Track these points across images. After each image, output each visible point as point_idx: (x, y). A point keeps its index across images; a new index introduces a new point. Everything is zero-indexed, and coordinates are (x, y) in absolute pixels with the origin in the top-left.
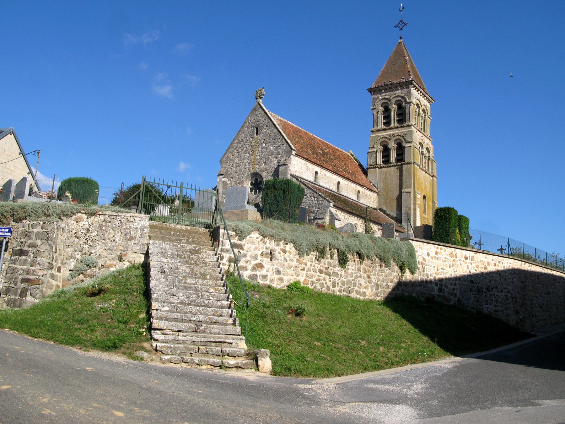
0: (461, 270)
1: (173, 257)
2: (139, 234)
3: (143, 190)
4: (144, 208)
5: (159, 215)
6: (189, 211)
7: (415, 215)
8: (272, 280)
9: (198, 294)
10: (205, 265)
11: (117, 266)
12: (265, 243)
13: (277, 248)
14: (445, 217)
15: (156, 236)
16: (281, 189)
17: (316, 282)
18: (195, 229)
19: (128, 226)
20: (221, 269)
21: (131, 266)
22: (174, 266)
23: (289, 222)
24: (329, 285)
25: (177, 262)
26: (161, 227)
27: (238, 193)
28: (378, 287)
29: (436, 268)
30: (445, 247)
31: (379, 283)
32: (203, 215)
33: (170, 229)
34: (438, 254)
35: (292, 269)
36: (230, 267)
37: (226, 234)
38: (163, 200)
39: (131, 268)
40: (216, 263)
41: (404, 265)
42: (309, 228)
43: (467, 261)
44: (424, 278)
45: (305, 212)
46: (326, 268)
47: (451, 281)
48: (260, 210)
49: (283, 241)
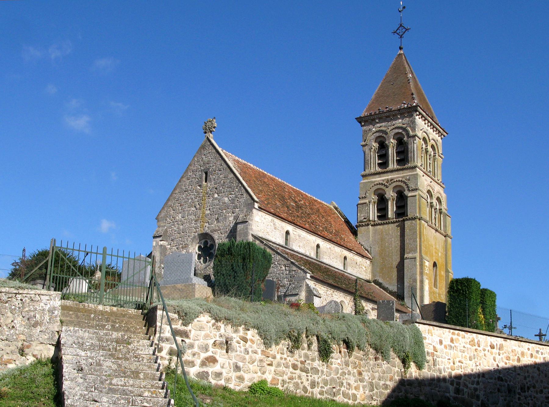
0: (485, 364)
1: (93, 349)
2: (47, 318)
3: (52, 257)
4: (53, 282)
5: (74, 292)
6: (115, 287)
7: (423, 289)
8: (229, 379)
9: (128, 400)
10: (137, 359)
11: (17, 362)
12: (218, 328)
13: (234, 335)
14: (463, 291)
15: (70, 321)
16: (240, 255)
17: (288, 381)
18: (124, 311)
19: (31, 307)
20: (159, 365)
21: (36, 361)
22: (94, 361)
23: (251, 301)
24: (306, 386)
25: (100, 355)
26: (77, 308)
27: (182, 261)
28: (373, 387)
29: (451, 361)
30: (463, 333)
31: (374, 381)
32: (134, 292)
33: (89, 312)
34: (454, 342)
35: (255, 364)
36: (171, 362)
37: (165, 316)
38: (79, 271)
39: (36, 364)
40: (152, 357)
41: (407, 356)
42: (279, 308)
43: (494, 351)
44: (435, 374)
45: (272, 286)
46: (302, 363)
47: (472, 378)
48: (211, 284)
49: (243, 326)
